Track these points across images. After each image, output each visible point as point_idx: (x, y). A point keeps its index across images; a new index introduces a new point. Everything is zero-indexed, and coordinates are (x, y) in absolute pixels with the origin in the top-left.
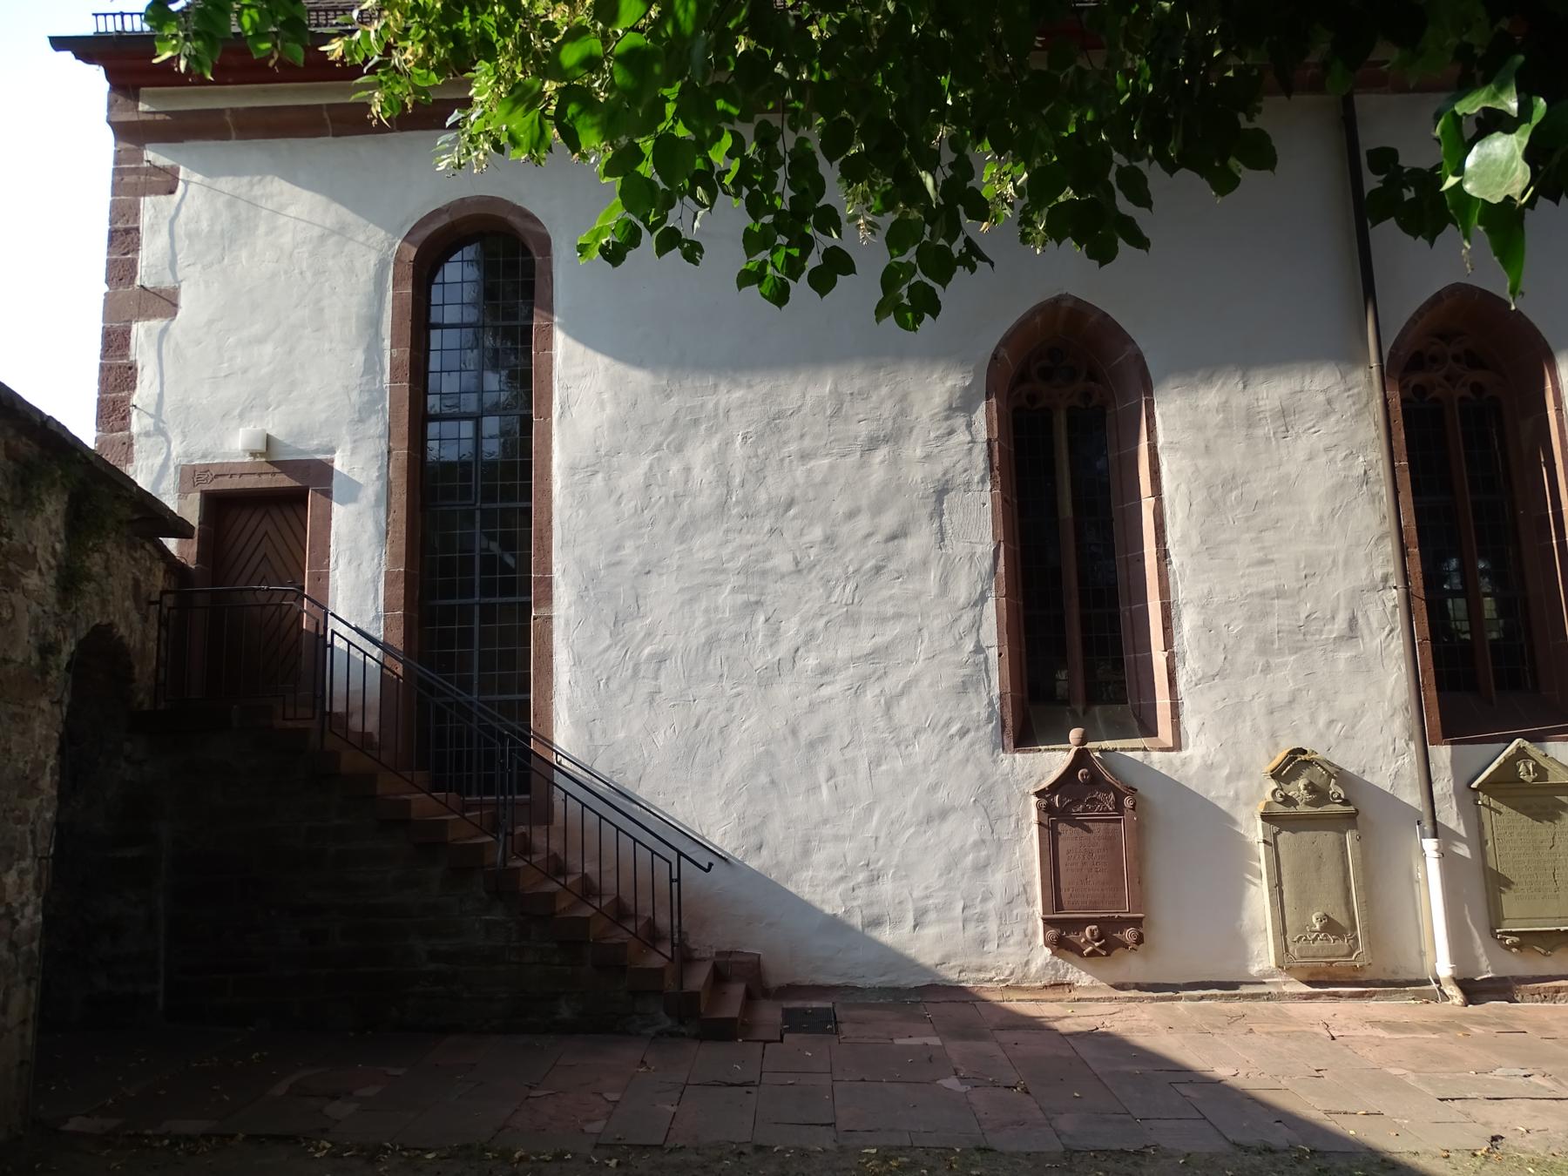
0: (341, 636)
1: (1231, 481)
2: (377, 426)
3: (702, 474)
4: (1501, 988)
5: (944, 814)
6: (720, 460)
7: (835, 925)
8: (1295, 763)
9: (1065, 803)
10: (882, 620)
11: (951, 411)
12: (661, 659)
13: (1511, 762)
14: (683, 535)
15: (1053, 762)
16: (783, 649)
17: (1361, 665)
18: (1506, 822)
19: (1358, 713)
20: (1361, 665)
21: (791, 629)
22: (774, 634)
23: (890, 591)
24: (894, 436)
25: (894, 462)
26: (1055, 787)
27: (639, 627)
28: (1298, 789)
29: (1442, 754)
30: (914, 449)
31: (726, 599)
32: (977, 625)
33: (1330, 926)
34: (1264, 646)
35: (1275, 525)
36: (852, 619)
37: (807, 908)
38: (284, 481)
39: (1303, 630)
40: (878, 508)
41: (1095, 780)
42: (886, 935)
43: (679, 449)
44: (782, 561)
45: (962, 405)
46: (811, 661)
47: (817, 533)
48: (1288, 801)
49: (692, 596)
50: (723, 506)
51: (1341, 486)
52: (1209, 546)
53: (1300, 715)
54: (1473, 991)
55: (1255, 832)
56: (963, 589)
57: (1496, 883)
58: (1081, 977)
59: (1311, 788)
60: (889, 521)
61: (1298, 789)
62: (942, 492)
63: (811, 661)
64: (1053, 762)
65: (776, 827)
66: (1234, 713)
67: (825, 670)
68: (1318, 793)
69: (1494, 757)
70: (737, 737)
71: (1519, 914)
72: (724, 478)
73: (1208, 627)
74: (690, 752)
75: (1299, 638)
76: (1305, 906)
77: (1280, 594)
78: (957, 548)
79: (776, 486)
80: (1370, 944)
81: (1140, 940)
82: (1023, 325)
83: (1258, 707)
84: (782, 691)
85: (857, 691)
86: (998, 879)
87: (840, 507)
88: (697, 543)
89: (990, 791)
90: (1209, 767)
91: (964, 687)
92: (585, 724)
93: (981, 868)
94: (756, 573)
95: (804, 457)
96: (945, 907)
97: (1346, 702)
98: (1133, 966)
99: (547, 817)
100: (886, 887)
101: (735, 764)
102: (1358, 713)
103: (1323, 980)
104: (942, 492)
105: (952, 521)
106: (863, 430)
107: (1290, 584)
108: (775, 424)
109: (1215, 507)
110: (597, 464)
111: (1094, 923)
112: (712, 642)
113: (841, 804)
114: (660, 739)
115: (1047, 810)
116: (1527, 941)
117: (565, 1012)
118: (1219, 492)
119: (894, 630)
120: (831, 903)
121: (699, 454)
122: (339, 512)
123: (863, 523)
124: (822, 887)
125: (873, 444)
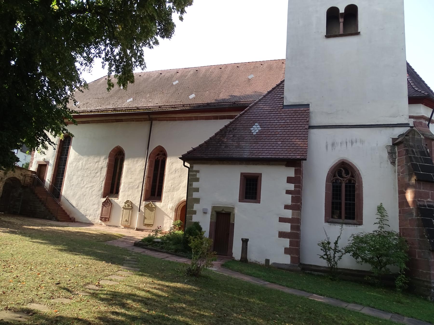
0: (47, 180)
1: (130, 169)
2: (54, 158)
3: (80, 165)
4: (142, 230)
5: (94, 204)
6: (82, 163)
7: (83, 215)
8: (127, 201)
9: (104, 204)
10: (93, 182)
11: (104, 159)
12: (73, 185)
13: (149, 204)
14: (78, 172)
15: (105, 199)
16: (84, 185)
17: (138, 191)
18: (148, 211)
19: (136, 197)
20: (138, 191)
21: (85, 183)
22: (83, 183)
23: (95, 179)
24: (98, 162)
25: (98, 165)
26: (104, 202)
27: (72, 181)
28: (126, 205)
29: (144, 203)
30: (100, 163)
31: (80, 179)
32: (102, 184)
33: (126, 220)
34: (129, 188)
35: (133, 174)
36: (91, 182)
37: (81, 213)
38: (45, 163)
39: (133, 187)
40: (95, 170)
41: (108, 202)
42: (87, 217)
43: (79, 162)
44: (86, 175)
45: (105, 159)
46: (86, 186)
47: (89, 172)
48: (125, 206)
49: (77, 178)
50: (81, 168)
51: (140, 170)
52: (126, 176)
53: (130, 197)
54: (137, 230)
55: (122, 209)
56: (101, 180)
57: (145, 218)
58: (103, 224)
59: (128, 205)
60: (96, 171)
61: (126, 205)
62: (102, 168)
63: (86, 186)
64: (105, 199)
65: (79, 204)
66: (124, 196)
67: (87, 188)
68: (128, 205)
69: (148, 203)
70: (78, 194)
71: (146, 222)
72: (82, 165)
73: (124, 186)
74: (73, 195)
75: (132, 188)
76: (124, 218)
77: (132, 182)
78: (102, 175)
79: (87, 167)
80: (130, 223)
81: (108, 220)
82: (114, 149)
83: (126, 195)
84: (83, 189)
85: (90, 190)
86: (98, 212)
87: (92, 169)
88: (79, 172)
89: (99, 202)
90: (120, 202)
91: (99, 190)
92: (65, 191)
93: (97, 211)
94: (83, 176)
95: (90, 163)
96: (92, 215)
97: (135, 195)
98: (108, 223)
99: (60, 201)
100: (88, 212)
101: (77, 197)
102: (136, 197)
103: (126, 227)
104: (102, 168)
105: (102, 172)
106: (96, 161)
107: (133, 181)
108: (88, 160)
109: (128, 172)
110: (71, 163)
111: (105, 219)
112: (78, 184)
113: (85, 202)
114: (71, 194)
115: (103, 204)
116: (145, 225)
117: (48, 217)
118: (129, 169)
119: (95, 183)
120: (83, 213)
121: (80, 162)
122: (49, 167)
123: (94, 171)
124: (82, 211)
125: (96, 162)
